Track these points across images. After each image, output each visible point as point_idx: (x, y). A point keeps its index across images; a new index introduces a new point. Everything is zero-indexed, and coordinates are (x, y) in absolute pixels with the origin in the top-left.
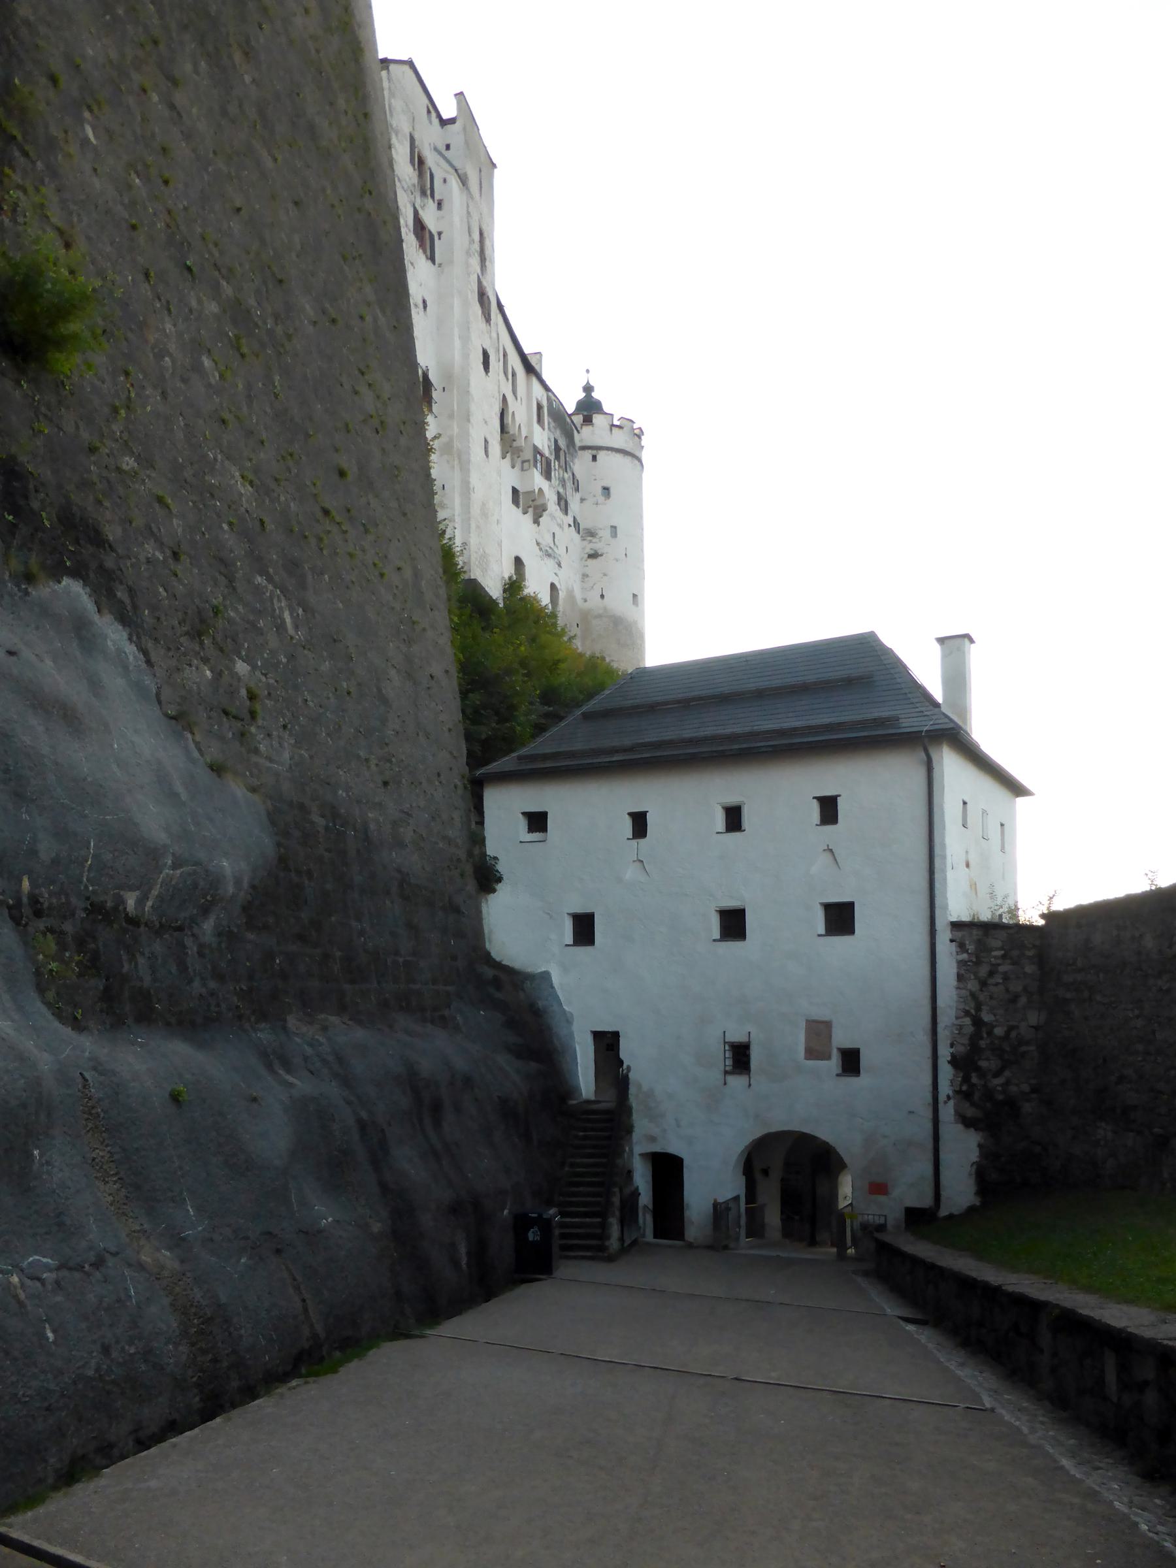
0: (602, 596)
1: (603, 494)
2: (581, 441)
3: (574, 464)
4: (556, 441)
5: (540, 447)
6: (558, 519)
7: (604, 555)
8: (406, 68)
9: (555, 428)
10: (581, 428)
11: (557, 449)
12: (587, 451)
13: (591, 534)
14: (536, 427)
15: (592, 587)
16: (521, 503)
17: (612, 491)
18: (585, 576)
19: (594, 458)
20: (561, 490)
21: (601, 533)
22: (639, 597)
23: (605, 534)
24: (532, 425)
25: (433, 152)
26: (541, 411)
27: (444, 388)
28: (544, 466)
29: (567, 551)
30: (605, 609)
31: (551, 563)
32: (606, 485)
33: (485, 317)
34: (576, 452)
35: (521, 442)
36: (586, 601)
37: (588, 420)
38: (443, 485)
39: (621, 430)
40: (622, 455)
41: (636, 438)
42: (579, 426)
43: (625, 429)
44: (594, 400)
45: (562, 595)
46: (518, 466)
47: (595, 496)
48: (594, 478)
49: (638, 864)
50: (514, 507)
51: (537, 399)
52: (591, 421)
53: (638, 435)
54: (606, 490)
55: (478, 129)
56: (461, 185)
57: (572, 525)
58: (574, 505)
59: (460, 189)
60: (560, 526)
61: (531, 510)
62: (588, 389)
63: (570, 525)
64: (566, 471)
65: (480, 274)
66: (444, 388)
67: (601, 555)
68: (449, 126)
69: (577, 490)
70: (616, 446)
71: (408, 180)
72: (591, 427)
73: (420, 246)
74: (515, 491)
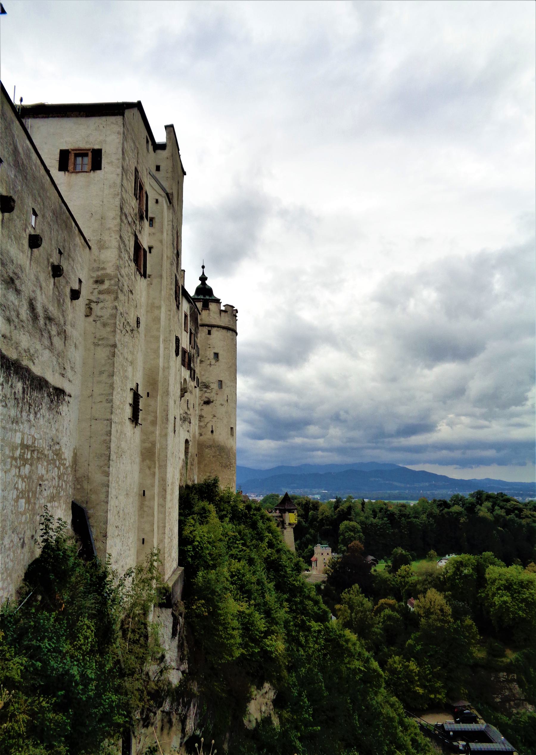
0: (212, 432)
1: (214, 358)
2: (201, 320)
8: (136, 111)
10: (202, 311)
18: (201, 417)
19: (209, 333)
23: (214, 386)
25: (149, 176)
32: (216, 351)
37: (206, 306)
38: (144, 491)
42: (200, 309)
44: (207, 287)
59: (168, 207)
62: (203, 279)
66: (148, 393)
67: (212, 402)
68: (159, 152)
69: (198, 356)
70: (223, 325)
71: (132, 211)
72: (208, 311)
73: (137, 269)
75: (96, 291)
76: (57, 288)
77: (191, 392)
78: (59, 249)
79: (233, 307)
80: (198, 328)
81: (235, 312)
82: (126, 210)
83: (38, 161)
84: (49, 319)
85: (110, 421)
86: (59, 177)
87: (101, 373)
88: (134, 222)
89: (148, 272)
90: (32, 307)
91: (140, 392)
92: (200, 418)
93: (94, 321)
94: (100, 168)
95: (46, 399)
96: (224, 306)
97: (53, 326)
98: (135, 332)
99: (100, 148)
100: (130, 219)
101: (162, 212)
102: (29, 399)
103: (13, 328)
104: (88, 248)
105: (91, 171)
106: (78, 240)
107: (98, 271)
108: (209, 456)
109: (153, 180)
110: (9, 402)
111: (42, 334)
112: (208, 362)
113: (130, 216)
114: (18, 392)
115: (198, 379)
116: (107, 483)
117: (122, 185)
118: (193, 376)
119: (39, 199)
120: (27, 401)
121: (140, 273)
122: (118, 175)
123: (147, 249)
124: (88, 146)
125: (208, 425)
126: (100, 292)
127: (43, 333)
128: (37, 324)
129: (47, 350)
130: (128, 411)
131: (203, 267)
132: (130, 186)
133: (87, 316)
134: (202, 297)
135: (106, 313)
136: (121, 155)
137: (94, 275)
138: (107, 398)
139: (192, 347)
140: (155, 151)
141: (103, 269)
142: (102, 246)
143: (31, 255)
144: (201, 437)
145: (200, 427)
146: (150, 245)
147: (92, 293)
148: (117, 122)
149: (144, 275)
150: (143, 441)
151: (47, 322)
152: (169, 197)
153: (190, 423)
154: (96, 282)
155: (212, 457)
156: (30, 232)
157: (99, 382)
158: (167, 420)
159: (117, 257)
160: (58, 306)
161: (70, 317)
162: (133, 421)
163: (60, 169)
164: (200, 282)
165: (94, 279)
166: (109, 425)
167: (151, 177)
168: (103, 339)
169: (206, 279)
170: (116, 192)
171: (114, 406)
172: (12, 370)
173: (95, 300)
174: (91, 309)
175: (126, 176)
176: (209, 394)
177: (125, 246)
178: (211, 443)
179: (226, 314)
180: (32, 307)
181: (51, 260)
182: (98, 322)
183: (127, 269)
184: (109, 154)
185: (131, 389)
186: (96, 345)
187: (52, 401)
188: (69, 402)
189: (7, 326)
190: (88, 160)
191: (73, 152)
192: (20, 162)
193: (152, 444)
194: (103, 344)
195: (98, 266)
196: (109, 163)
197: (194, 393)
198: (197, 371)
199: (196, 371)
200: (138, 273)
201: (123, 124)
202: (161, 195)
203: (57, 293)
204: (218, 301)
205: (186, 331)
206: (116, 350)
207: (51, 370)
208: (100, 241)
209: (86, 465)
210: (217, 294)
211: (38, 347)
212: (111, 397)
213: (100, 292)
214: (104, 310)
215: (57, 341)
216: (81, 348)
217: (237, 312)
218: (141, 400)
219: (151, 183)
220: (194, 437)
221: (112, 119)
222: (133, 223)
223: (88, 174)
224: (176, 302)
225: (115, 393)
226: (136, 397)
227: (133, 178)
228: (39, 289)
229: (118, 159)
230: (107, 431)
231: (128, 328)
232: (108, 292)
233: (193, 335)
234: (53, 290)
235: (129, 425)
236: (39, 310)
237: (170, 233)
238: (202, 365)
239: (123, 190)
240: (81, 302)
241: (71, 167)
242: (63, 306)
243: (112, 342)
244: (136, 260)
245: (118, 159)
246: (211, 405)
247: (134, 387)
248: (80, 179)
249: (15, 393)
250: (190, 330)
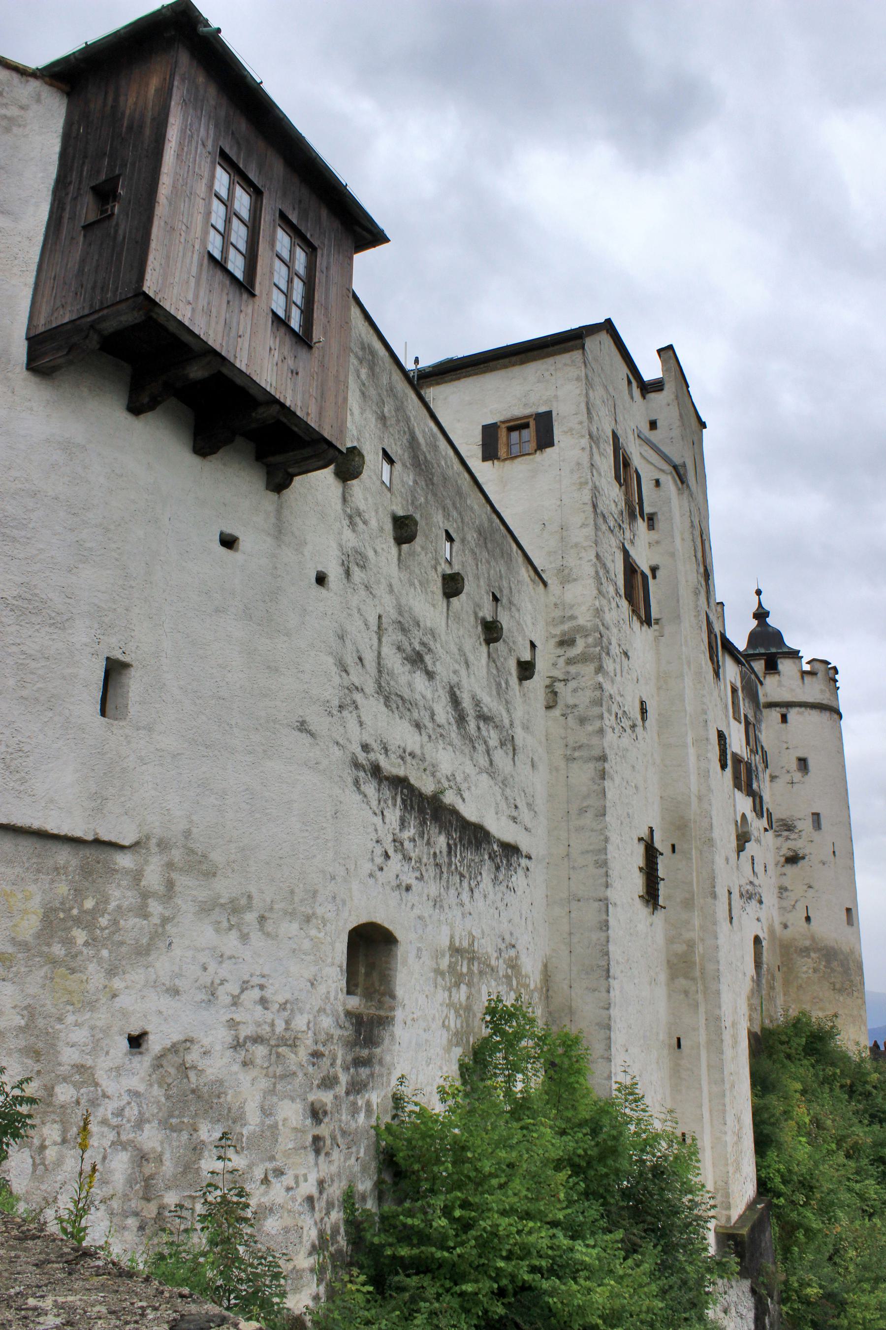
0: (808, 919)
2: (765, 695)
5: (739, 752)
7: (807, 858)
8: (604, 338)
10: (765, 677)
13: (788, 827)
15: (794, 906)
17: (811, 763)
18: (783, 889)
19: (784, 719)
21: (800, 825)
22: (854, 911)
25: (638, 441)
27: (673, 846)
30: (813, 939)
32: (801, 755)
36: (786, 926)
37: (772, 666)
38: (679, 1039)
40: (818, 711)
42: (761, 675)
43: (819, 675)
44: (770, 630)
48: (785, 746)
51: (731, 682)
56: (679, 482)
59: (679, 489)
62: (761, 615)
66: (673, 846)
67: (803, 858)
68: (652, 396)
69: (767, 767)
70: (810, 700)
71: (613, 506)
72: (777, 676)
73: (633, 611)
75: (561, 661)
76: (494, 661)
77: (758, 841)
78: (493, 593)
79: (827, 663)
80: (761, 712)
81: (832, 672)
82: (601, 507)
83: (451, 452)
84: (484, 718)
85: (605, 903)
86: (484, 471)
87: (583, 811)
88: (620, 526)
89: (654, 615)
90: (455, 701)
91: (658, 844)
92: (782, 893)
93: (563, 715)
94: (551, 444)
95: (488, 865)
96: (808, 663)
97: (492, 732)
98: (639, 729)
99: (548, 410)
100: (612, 523)
101: (669, 501)
102: (458, 864)
103: (425, 738)
104: (541, 585)
105: (536, 451)
106: (524, 573)
107: (562, 622)
108: (805, 969)
109: (647, 448)
110: (427, 870)
111: (474, 747)
112: (788, 778)
113: (611, 518)
114: (441, 852)
115: (770, 815)
116: (606, 1021)
117: (592, 465)
118: (759, 808)
119: (455, 514)
120: (456, 868)
121: (639, 617)
122: (583, 449)
123: (648, 572)
124: (528, 411)
125: (798, 905)
126: (570, 662)
127: (477, 745)
128: (465, 729)
129: (485, 775)
130: (638, 883)
131: (759, 592)
132: (606, 464)
133: (549, 707)
134: (763, 651)
135: (583, 699)
136: (586, 415)
137: (557, 631)
138: (596, 858)
139: (751, 751)
140: (644, 397)
141: (573, 618)
142: (566, 577)
143: (448, 610)
145: (782, 909)
146: (653, 563)
147: (555, 665)
148: (573, 361)
149: (647, 621)
150: (670, 941)
151: (482, 724)
152: (679, 473)
153: (761, 902)
154: (562, 643)
155: (810, 971)
156: (443, 570)
157: (580, 829)
158: (714, 896)
159: (595, 592)
160: (499, 694)
161: (519, 714)
162: (648, 901)
163: (485, 459)
164: (756, 622)
165: (557, 640)
166: (604, 909)
167: (642, 443)
168: (580, 747)
169: (767, 614)
170: (583, 480)
171: (610, 872)
172: (427, 814)
173: (561, 677)
174: (555, 694)
175: (598, 448)
176: (794, 842)
177: (608, 572)
178: (807, 943)
179: (814, 679)
180: (455, 701)
181: (481, 614)
182: (570, 717)
183: (614, 613)
184: (565, 417)
185: (640, 839)
186: (570, 759)
187: (498, 868)
188: (528, 869)
189: (417, 737)
190: (529, 435)
191: (503, 426)
192: (421, 458)
193: (688, 946)
194: (581, 757)
195: (562, 614)
196: (565, 432)
197: (763, 842)
198: (766, 797)
199: (764, 798)
200: (635, 618)
201: (585, 363)
202: (663, 471)
203: (495, 672)
204: (794, 655)
205: (737, 719)
206: (607, 765)
207: (493, 811)
208: (561, 570)
209: (566, 987)
210: (791, 641)
211: (469, 769)
212: (603, 857)
213: (570, 662)
214: (580, 693)
215: (501, 758)
216: (542, 767)
217: (837, 672)
218: (660, 860)
219: (644, 453)
220: (772, 931)
221: (565, 358)
222: (617, 529)
223: (531, 457)
224: (713, 664)
225: (610, 848)
226: (651, 854)
227: (610, 450)
228: (464, 666)
229: (581, 423)
230: (600, 922)
231: (626, 723)
232: (584, 658)
233: (751, 727)
234: (488, 665)
235: (641, 910)
236: (467, 704)
237: (687, 536)
238: (774, 784)
239: (595, 473)
240: (537, 683)
241: (502, 452)
242: (506, 693)
243: (596, 752)
244: (630, 596)
245: (581, 423)
246: (801, 863)
247: (644, 833)
248: (518, 468)
249: (435, 854)
250: (746, 716)
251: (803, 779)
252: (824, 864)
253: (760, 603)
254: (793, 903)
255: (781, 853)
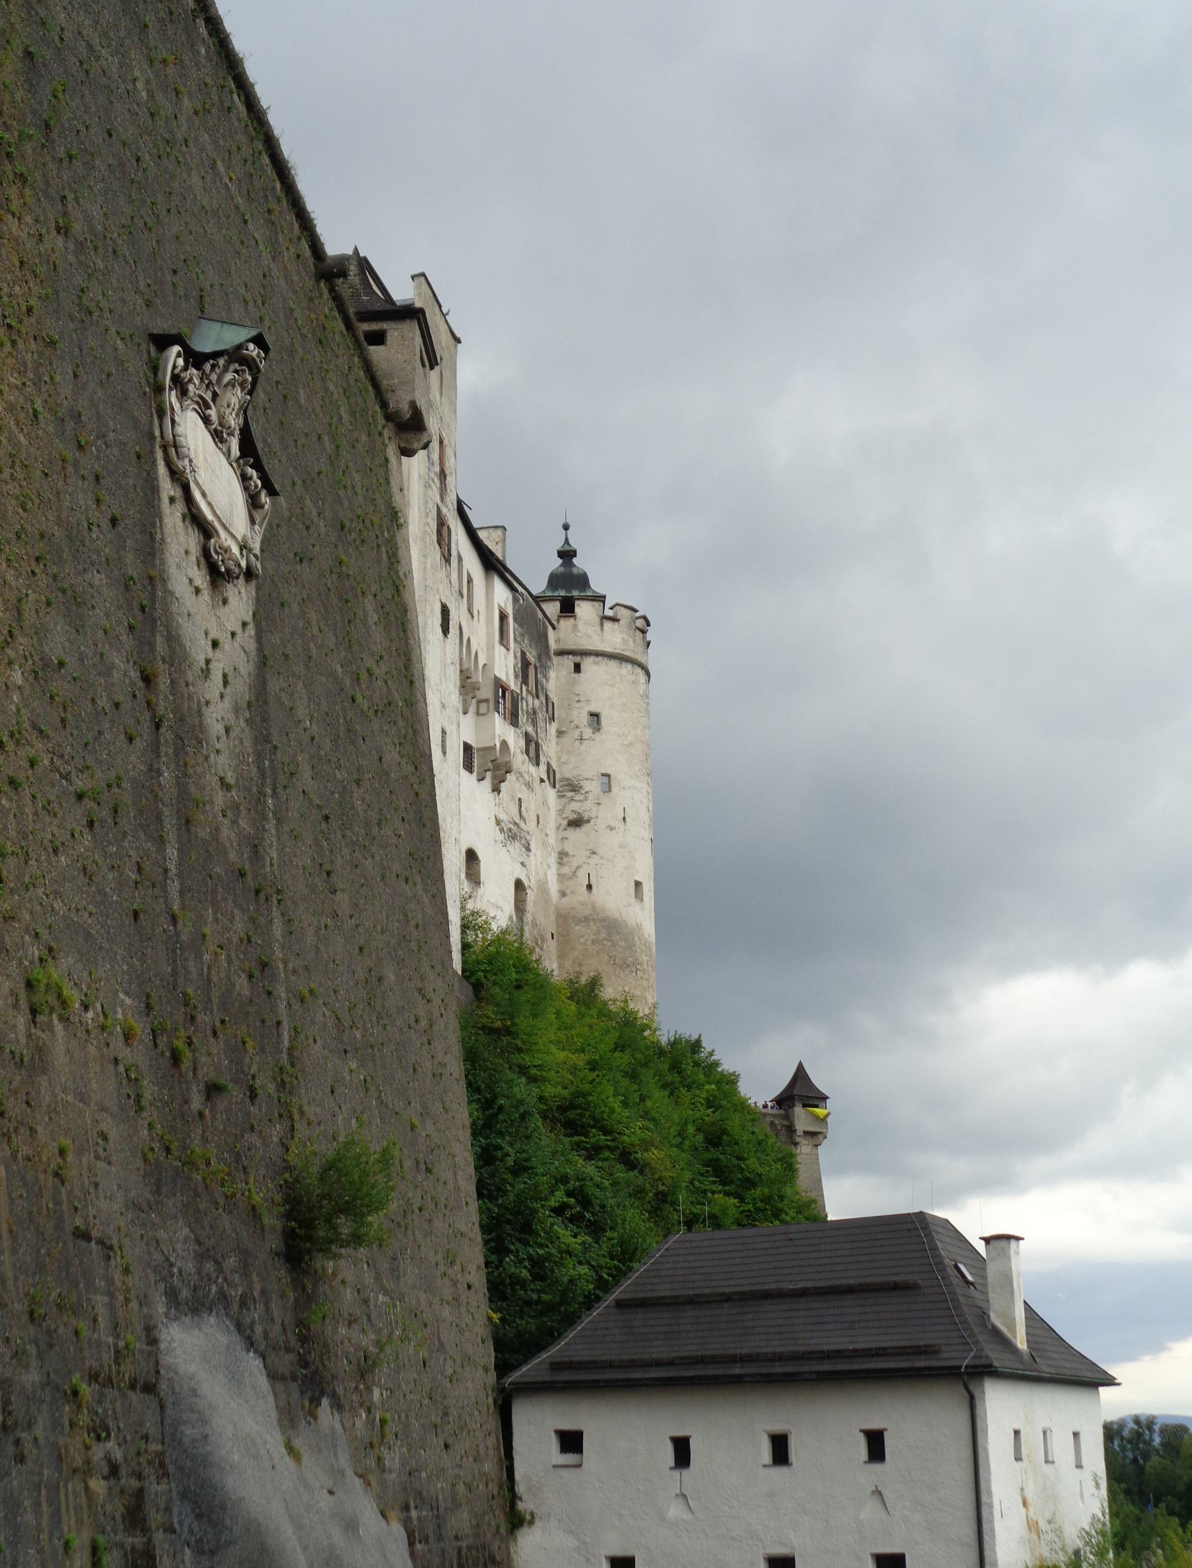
0: (589, 887)
3: (547, 680)
4: (523, 654)
5: (503, 677)
6: (525, 775)
7: (592, 821)
9: (522, 635)
10: (558, 621)
11: (525, 664)
12: (566, 656)
13: (573, 787)
14: (500, 650)
16: (475, 769)
17: (604, 721)
18: (562, 855)
19: (577, 668)
20: (530, 729)
21: (587, 786)
23: (593, 787)
24: (493, 648)
26: (505, 622)
28: (508, 705)
29: (538, 822)
31: (516, 847)
33: (444, 557)
34: (550, 659)
35: (479, 677)
37: (568, 608)
39: (617, 623)
41: (639, 634)
45: (531, 896)
46: (472, 709)
47: (577, 727)
49: (681, 1500)
50: (464, 773)
51: (499, 606)
52: (573, 611)
53: (643, 626)
54: (595, 716)
55: (440, 307)
57: (545, 778)
58: (550, 748)
60: (528, 785)
61: (489, 774)
62: (567, 555)
63: (542, 781)
64: (538, 697)
65: (439, 502)
67: (588, 821)
70: (609, 649)
72: (572, 620)
74: (467, 748)
79: (636, 611)
92: (561, 859)
96: (611, 608)
108: (582, 940)
112: (576, 734)
125: (579, 873)
131: (566, 527)
144: (564, 900)
155: (589, 943)
164: (560, 561)
169: (573, 554)
176: (579, 804)
178: (587, 913)
179: (616, 625)
246: (585, 828)
251: (593, 736)
252: (611, 829)
253: (567, 541)
254: (574, 869)
255: (564, 816)
